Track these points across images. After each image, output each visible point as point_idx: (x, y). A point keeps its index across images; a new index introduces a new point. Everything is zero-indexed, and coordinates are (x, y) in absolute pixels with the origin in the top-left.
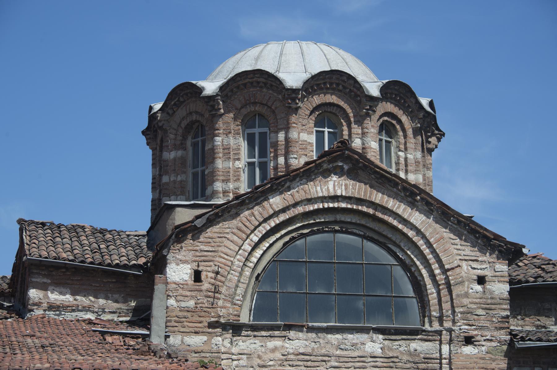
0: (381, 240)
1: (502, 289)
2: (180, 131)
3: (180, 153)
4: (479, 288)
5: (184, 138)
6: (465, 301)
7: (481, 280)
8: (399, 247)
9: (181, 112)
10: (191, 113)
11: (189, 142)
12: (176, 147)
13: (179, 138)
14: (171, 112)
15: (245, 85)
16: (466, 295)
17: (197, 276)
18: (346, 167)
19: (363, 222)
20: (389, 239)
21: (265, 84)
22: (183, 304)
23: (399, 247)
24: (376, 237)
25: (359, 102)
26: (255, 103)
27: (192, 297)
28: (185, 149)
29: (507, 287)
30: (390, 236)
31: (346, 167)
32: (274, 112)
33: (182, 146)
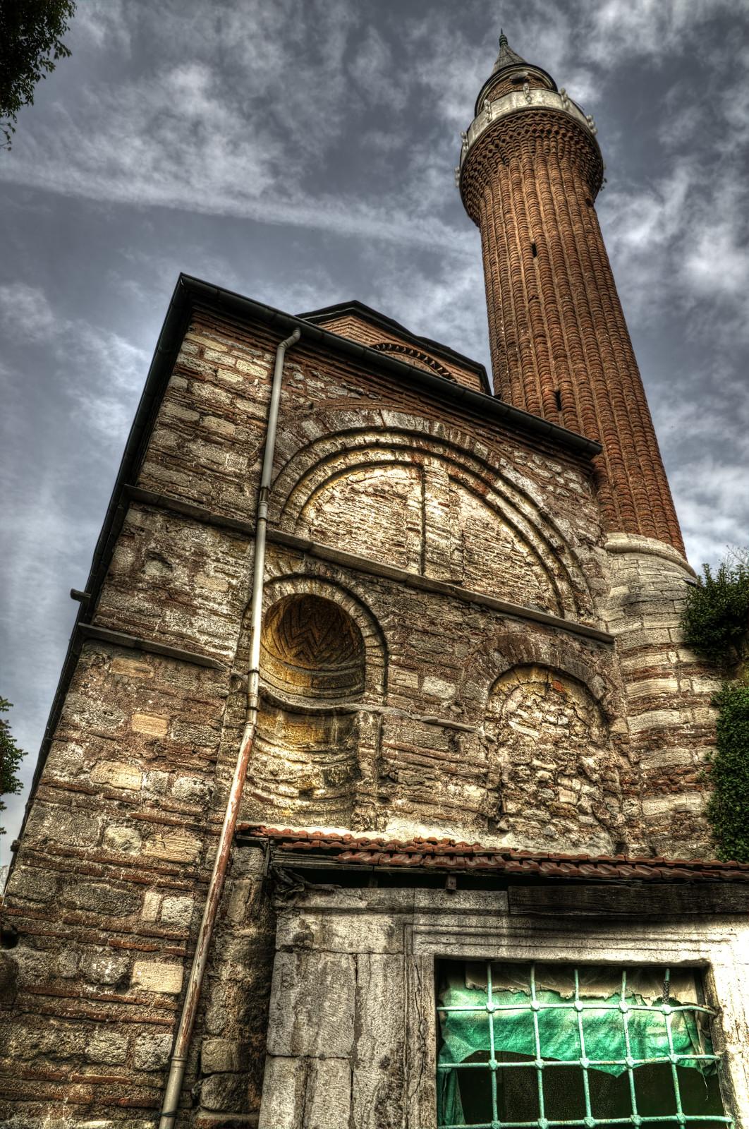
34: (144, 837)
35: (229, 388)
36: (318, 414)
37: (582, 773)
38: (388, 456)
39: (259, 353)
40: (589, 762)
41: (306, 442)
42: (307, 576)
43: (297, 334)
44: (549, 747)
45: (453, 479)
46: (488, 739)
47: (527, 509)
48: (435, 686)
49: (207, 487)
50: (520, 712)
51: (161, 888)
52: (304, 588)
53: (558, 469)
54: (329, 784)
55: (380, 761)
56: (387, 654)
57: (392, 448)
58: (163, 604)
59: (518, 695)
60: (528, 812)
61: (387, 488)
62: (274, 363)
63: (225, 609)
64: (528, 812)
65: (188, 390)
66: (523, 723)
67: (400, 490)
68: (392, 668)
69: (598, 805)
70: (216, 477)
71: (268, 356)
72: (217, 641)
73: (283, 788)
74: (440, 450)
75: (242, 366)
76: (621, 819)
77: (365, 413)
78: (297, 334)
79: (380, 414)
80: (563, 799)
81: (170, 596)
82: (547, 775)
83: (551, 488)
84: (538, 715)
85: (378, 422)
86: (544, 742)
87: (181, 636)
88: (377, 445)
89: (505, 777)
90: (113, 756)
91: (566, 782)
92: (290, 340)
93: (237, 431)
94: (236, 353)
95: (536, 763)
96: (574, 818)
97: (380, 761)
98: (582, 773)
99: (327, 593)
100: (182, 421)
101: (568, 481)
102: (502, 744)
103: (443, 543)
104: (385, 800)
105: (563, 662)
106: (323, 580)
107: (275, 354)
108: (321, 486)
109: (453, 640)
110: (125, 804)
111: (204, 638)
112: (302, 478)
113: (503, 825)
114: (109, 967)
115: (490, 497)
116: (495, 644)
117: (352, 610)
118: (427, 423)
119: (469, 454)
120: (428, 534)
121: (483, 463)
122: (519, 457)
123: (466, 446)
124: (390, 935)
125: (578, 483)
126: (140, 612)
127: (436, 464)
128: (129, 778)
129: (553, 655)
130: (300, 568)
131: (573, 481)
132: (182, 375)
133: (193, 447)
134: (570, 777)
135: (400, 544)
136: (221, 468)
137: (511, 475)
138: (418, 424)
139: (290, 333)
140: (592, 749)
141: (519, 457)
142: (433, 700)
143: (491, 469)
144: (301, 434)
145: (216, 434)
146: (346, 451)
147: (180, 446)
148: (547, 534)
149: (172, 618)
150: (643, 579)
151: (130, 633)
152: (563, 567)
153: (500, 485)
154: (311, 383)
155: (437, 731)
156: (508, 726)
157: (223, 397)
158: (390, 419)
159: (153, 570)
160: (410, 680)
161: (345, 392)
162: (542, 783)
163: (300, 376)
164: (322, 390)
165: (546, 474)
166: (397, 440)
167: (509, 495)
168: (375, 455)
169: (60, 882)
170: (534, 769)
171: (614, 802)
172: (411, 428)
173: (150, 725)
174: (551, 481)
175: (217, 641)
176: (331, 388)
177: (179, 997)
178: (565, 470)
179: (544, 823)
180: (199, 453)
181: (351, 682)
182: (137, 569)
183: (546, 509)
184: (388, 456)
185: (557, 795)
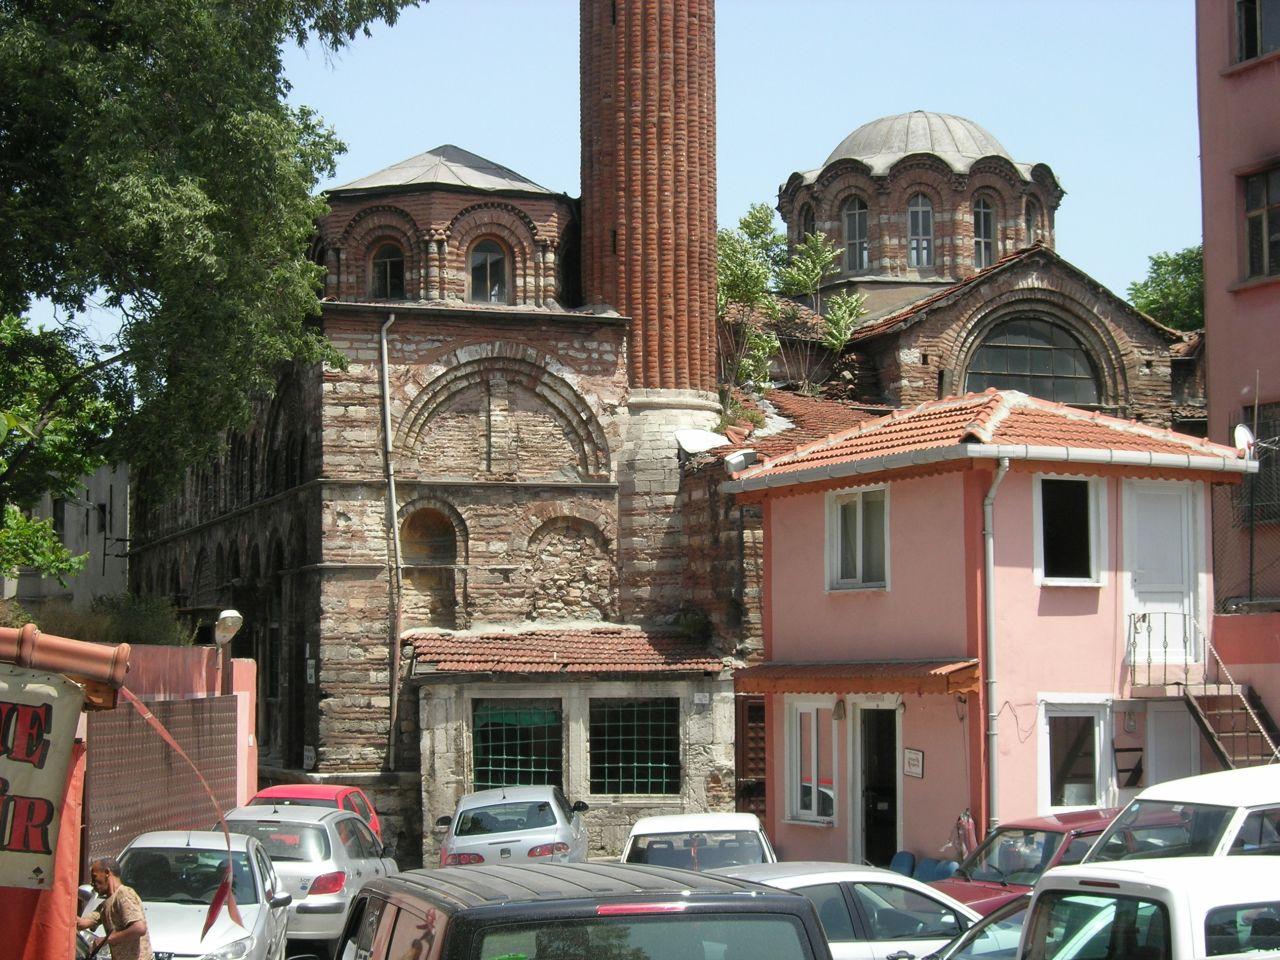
0: (1067, 327)
1: (1165, 371)
2: (837, 203)
3: (836, 224)
4: (1147, 371)
5: (840, 209)
6: (1137, 383)
7: (1149, 364)
8: (1082, 333)
9: (837, 186)
10: (849, 187)
11: (844, 213)
12: (830, 218)
13: (835, 209)
14: (826, 183)
15: (911, 166)
16: (1137, 377)
17: (925, 358)
18: (1042, 262)
19: (1053, 311)
20: (1075, 328)
21: (931, 166)
22: (915, 385)
23: (1082, 333)
24: (1063, 324)
25: (1013, 186)
26: (920, 183)
27: (922, 379)
28: (840, 220)
29: (1169, 370)
30: (1074, 323)
31: (1042, 262)
32: (938, 193)
33: (838, 218)
34: (366, 650)
35: (358, 380)
36: (414, 376)
37: (586, 578)
38: (464, 383)
39: (370, 337)
40: (591, 570)
41: (409, 403)
42: (421, 498)
43: (393, 318)
44: (567, 565)
45: (511, 383)
46: (528, 571)
47: (565, 392)
48: (497, 546)
49: (358, 459)
50: (549, 548)
51: (375, 670)
52: (419, 505)
53: (594, 345)
54: (444, 606)
55: (466, 596)
56: (467, 534)
57: (466, 377)
58: (350, 540)
59: (547, 539)
60: (550, 605)
61: (464, 408)
62: (380, 343)
63: (381, 534)
64: (550, 605)
65: (335, 392)
66: (552, 555)
67: (474, 408)
68: (470, 542)
69: (593, 595)
70: (362, 452)
71: (376, 336)
72: (379, 553)
73: (422, 610)
74: (500, 365)
75: (363, 355)
76: (607, 601)
77: (445, 358)
78: (393, 318)
79: (456, 355)
80: (572, 594)
81: (354, 535)
82: (563, 582)
83: (585, 368)
84: (560, 547)
85: (455, 363)
86: (562, 563)
87: (362, 556)
88: (457, 379)
89: (537, 589)
90: (345, 620)
91: (574, 584)
92: (389, 323)
93: (368, 412)
94: (356, 345)
95: (556, 577)
96: (578, 603)
97: (466, 596)
98: (586, 578)
99: (431, 505)
100: (336, 418)
101: (601, 354)
102: (536, 570)
103: (502, 442)
104: (470, 614)
105: (578, 511)
106: (429, 498)
107: (380, 332)
108: (423, 425)
109: (506, 515)
110: (354, 640)
111: (373, 553)
112: (410, 430)
113: (535, 614)
114: (363, 701)
115: (538, 390)
116: (533, 512)
117: (446, 512)
118: (489, 347)
119: (522, 361)
120: (493, 439)
121: (533, 365)
122: (562, 349)
123: (519, 357)
124: (456, 692)
125: (611, 352)
126: (341, 548)
127: (498, 375)
128: (354, 628)
129: (571, 509)
130: (415, 496)
131: (607, 352)
132: (328, 381)
133: (345, 434)
134: (578, 581)
135: (475, 450)
136: (363, 444)
137: (553, 369)
138: (484, 351)
139: (388, 318)
140: (593, 561)
141: (562, 349)
142: (494, 556)
143: (539, 367)
144: (405, 398)
145: (355, 421)
146: (435, 395)
147: (338, 437)
148: (579, 409)
149: (355, 544)
150: (645, 437)
151: (338, 561)
152: (589, 434)
153: (546, 379)
154: (407, 348)
155: (497, 574)
156: (540, 558)
157: (355, 386)
158: (463, 356)
159: (342, 523)
160: (481, 547)
161: (428, 346)
162: (560, 588)
163: (399, 346)
164: (416, 351)
165: (584, 356)
166: (469, 369)
167: (552, 385)
168: (454, 388)
169: (338, 675)
170: (555, 581)
171: (604, 591)
172: (478, 357)
173: (357, 604)
174: (589, 361)
175: (379, 553)
176: (421, 346)
177: (390, 708)
178: (600, 344)
179: (559, 610)
180: (349, 438)
181: (450, 552)
182: (335, 524)
183: (580, 391)
184: (464, 383)
185: (568, 593)
